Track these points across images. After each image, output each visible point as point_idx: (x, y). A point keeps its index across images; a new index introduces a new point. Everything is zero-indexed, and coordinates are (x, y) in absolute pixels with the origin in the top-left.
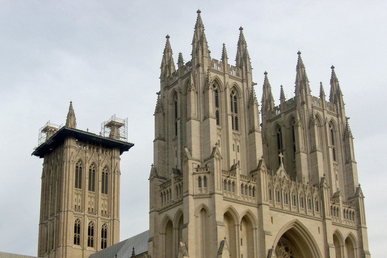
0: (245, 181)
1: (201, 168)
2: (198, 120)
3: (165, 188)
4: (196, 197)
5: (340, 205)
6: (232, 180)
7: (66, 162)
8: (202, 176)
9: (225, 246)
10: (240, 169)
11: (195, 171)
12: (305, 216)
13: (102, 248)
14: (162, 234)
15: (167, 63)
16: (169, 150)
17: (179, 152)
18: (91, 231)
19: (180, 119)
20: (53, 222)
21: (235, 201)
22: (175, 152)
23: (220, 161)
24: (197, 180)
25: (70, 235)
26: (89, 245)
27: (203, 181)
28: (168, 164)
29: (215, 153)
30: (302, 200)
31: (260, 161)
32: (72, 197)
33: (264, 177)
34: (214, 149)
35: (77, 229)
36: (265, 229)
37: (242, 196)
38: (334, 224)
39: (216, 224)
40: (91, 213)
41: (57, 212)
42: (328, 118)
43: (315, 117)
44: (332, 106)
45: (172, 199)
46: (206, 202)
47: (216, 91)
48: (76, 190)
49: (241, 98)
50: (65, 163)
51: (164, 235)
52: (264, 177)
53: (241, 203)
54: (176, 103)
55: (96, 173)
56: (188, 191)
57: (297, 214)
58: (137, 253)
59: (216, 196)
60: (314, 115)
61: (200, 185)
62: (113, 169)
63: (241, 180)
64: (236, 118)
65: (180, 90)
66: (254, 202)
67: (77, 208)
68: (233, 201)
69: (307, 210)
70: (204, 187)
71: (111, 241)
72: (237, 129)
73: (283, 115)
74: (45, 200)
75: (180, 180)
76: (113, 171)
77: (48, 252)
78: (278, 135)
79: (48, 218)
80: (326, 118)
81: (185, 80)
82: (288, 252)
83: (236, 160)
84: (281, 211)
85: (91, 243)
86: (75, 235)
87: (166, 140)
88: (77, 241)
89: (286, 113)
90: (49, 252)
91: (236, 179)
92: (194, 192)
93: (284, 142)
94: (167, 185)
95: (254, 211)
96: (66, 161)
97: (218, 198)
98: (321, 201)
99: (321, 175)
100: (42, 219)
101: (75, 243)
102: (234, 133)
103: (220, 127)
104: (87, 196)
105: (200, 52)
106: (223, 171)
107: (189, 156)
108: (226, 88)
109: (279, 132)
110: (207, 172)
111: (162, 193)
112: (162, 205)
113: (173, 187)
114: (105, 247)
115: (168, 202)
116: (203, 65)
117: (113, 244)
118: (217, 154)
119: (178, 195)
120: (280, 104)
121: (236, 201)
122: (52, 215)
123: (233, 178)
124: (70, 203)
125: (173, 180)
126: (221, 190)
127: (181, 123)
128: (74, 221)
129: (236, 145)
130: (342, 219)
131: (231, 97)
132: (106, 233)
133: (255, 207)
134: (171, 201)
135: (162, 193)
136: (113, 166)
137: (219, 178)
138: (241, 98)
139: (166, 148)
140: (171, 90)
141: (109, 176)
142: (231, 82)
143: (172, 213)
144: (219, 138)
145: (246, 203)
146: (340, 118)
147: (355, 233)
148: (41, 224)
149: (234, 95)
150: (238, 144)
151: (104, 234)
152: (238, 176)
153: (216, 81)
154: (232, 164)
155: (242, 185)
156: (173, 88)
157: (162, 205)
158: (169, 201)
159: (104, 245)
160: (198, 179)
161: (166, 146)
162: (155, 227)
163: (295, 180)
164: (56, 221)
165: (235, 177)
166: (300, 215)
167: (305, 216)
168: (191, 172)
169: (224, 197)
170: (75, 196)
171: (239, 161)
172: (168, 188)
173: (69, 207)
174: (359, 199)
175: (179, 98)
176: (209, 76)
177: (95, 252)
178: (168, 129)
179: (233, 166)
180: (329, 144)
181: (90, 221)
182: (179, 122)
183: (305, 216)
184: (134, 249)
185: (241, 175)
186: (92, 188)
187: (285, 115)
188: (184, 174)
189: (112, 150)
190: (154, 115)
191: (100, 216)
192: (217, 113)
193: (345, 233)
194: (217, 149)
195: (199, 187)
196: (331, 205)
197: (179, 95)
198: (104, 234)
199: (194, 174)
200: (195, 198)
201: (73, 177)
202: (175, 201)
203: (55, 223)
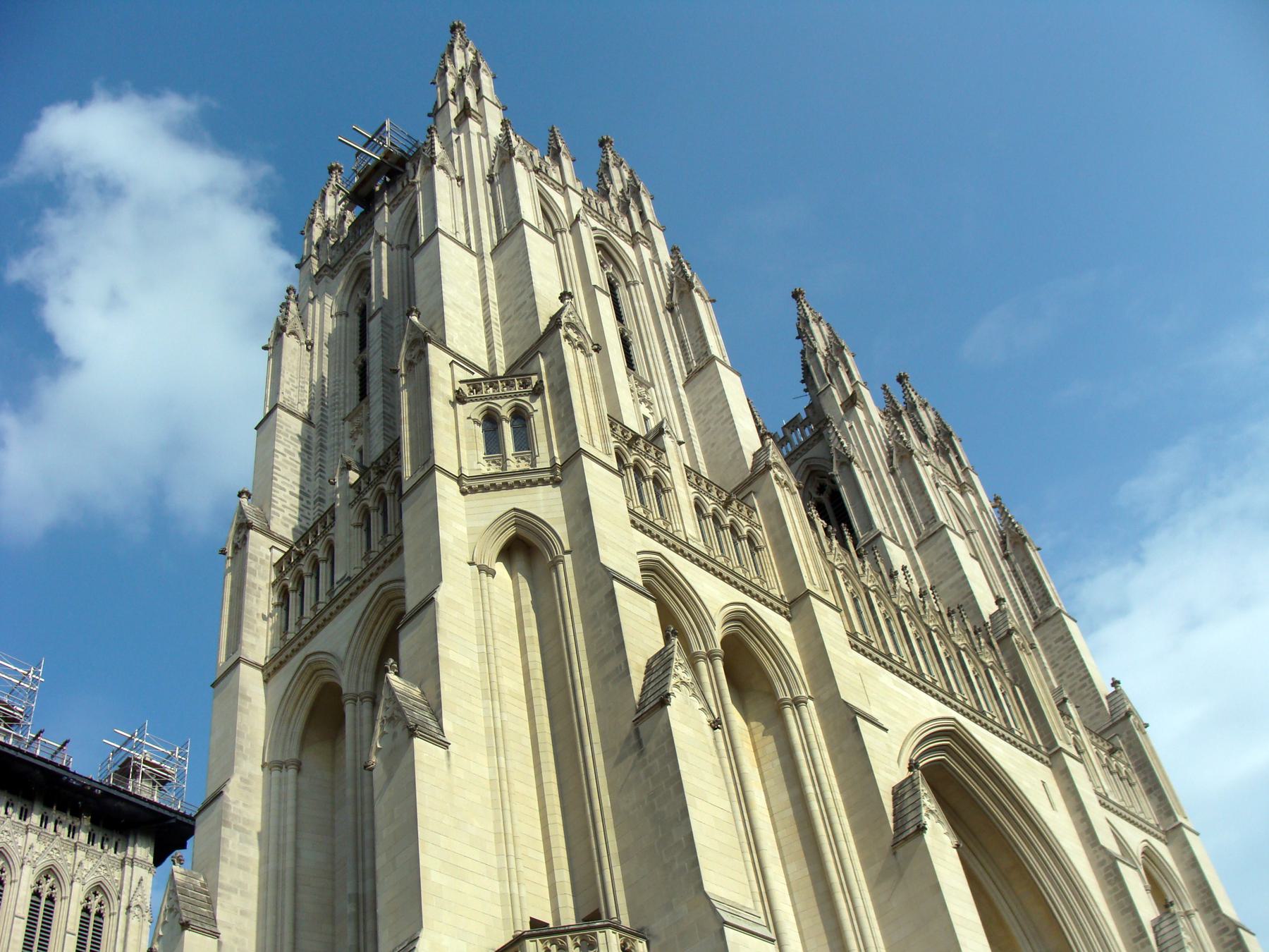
8: (504, 408)
10: (680, 443)
16: (328, 454)
24: (475, 422)
27: (507, 429)
49: (635, 283)
62: (125, 897)
76: (124, 904)
92: (464, 464)
98: (1017, 689)
136: (125, 890)
139: (313, 447)
189: (127, 837)
190: (265, 348)
199: (460, 398)
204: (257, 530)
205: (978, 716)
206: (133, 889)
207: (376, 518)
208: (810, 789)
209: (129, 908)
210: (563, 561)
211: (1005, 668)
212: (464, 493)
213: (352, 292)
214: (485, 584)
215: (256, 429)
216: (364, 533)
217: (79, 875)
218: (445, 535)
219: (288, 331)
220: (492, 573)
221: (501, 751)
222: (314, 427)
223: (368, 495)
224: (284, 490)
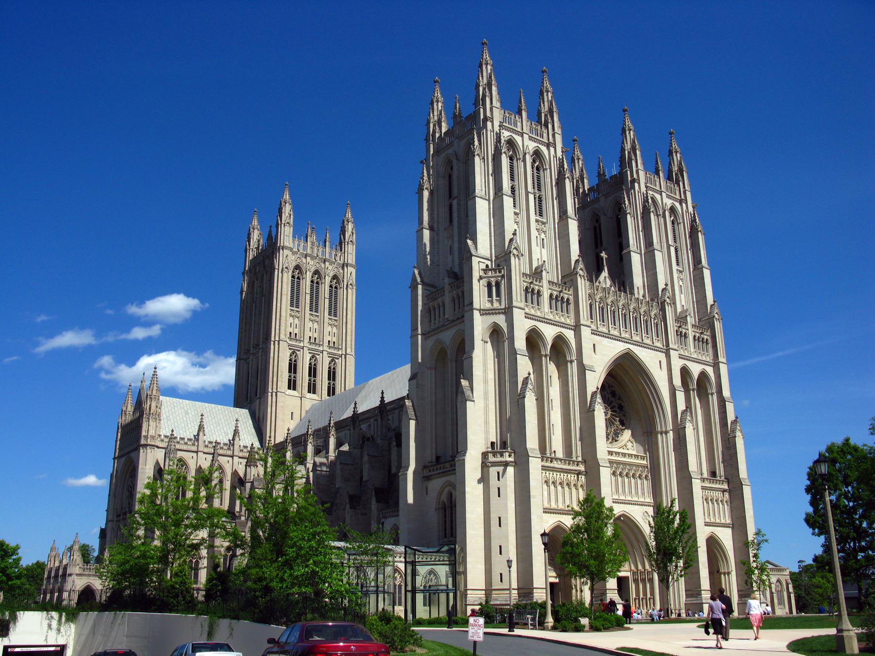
0: (555, 291)
1: (491, 270)
2: (486, 199)
3: (435, 299)
4: (484, 312)
5: (688, 330)
6: (537, 288)
7: (278, 270)
8: (493, 280)
9: (530, 386)
11: (482, 273)
12: (641, 344)
13: (329, 395)
14: (431, 368)
15: (436, 118)
17: (456, 246)
18: (313, 371)
20: (257, 358)
21: (541, 319)
22: (449, 247)
23: (519, 259)
24: (485, 286)
25: (282, 375)
26: (309, 392)
27: (494, 289)
28: (438, 265)
29: (513, 247)
30: (636, 321)
31: (577, 261)
32: (286, 320)
33: (582, 284)
34: (511, 240)
35: (293, 367)
36: (586, 362)
37: (551, 312)
38: (681, 357)
39: (514, 353)
40: (313, 343)
41: (263, 342)
42: (668, 204)
43: (650, 201)
44: (673, 185)
45: (446, 316)
46: (501, 320)
47: (511, 158)
48: (292, 310)
50: (276, 270)
51: (433, 371)
52: (582, 284)
53: (550, 322)
54: (450, 176)
55: (321, 287)
56: (471, 303)
57: (630, 341)
58: (387, 400)
59: (516, 311)
60: (649, 197)
61: (490, 295)
63: (550, 289)
64: (540, 198)
65: (456, 155)
66: (568, 322)
67: (293, 336)
68: (539, 319)
69: (644, 335)
70: (496, 297)
71: (343, 385)
72: (541, 215)
73: (602, 199)
74: (246, 325)
75: (459, 287)
76: (345, 283)
77: (249, 400)
78: (595, 228)
79: (249, 351)
80: (666, 204)
81: (464, 142)
82: (615, 397)
83: (540, 260)
84: (608, 336)
85: (312, 389)
86: (290, 376)
87: (435, 229)
88: (292, 385)
89: (606, 196)
90: (250, 401)
91: (542, 287)
93: (604, 238)
94: (437, 295)
95: (570, 335)
96: (277, 268)
97: (518, 315)
99: (661, 286)
100: (240, 353)
101: (289, 388)
102: (537, 221)
103: (517, 211)
104: (307, 320)
105: (488, 100)
106: (523, 274)
107: (473, 251)
108: (526, 154)
109: (596, 225)
110: (501, 275)
111: (429, 308)
112: (430, 326)
113: (447, 298)
114: (334, 394)
115: (439, 322)
116: (493, 119)
117: (345, 390)
118: (515, 248)
119: (455, 311)
120: (597, 182)
121: (543, 320)
122: (255, 346)
123: (538, 286)
124: (283, 328)
125: (447, 288)
126: (521, 301)
127: (458, 204)
128: (289, 356)
129: (540, 237)
130: (692, 350)
131: (533, 168)
132: (334, 373)
133: (570, 329)
134: (444, 319)
135: (429, 308)
136: (345, 277)
137: (518, 285)
138: (546, 169)
140: (443, 155)
141: (340, 291)
142: (531, 146)
143: (447, 336)
144: (516, 227)
145: (557, 324)
146: (684, 205)
147: (710, 370)
148: (239, 359)
149: (536, 165)
150: (543, 236)
151: (332, 375)
152: (545, 282)
153: (511, 143)
154: (535, 265)
155: (551, 295)
156: (446, 153)
157: (430, 326)
158: (441, 320)
159: (331, 391)
160: (486, 285)
161: (436, 238)
163: (625, 292)
164: (262, 356)
165: (540, 284)
166: (634, 343)
167: (641, 344)
168: (476, 274)
169: (526, 313)
170: (291, 320)
171: (544, 261)
172: (440, 300)
173: (281, 335)
174: (715, 321)
175: (455, 168)
176: (501, 134)
177: (316, 402)
178: (438, 214)
179: (536, 269)
180: (671, 242)
181: (311, 355)
182: (455, 202)
183: (641, 344)
184: (382, 393)
185: (549, 282)
186: (314, 306)
187: (606, 198)
188: (466, 278)
191: (326, 348)
192: (513, 189)
193: (695, 370)
194: (514, 241)
195: (488, 297)
196: (676, 328)
197: (455, 162)
198: (332, 375)
201: (288, 291)
202: (451, 319)
203: (260, 357)
206: (348, 277)
207: (456, 301)
208: (570, 390)
209: (347, 285)
212: (481, 315)
217: (327, 273)
218: (476, 333)
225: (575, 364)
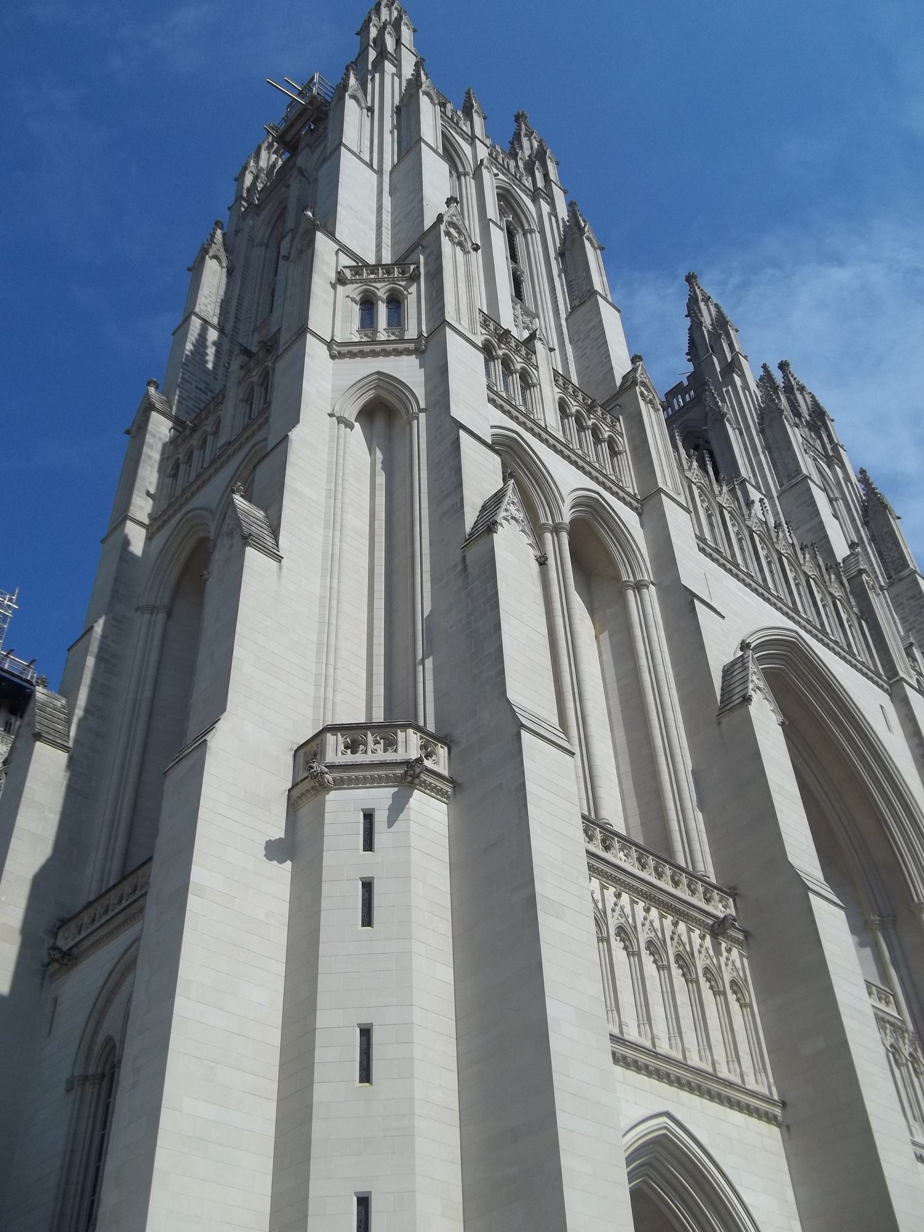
8: (382, 290)
10: (552, 350)
14: (153, 609)
19: (292, 230)
24: (353, 300)
27: (382, 310)
98: (863, 623)
162: (117, 580)
199: (341, 280)
200: (341, 356)
204: (159, 411)
205: (821, 634)
208: (643, 662)
210: (418, 418)
211: (853, 603)
212: (333, 357)
213: (274, 226)
214: (342, 433)
215: (173, 335)
216: (248, 406)
219: (210, 254)
220: (352, 427)
221: (336, 574)
222: (226, 336)
223: (254, 373)
224: (190, 383)
225: (651, 594)
